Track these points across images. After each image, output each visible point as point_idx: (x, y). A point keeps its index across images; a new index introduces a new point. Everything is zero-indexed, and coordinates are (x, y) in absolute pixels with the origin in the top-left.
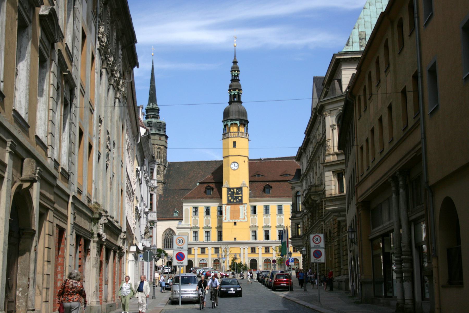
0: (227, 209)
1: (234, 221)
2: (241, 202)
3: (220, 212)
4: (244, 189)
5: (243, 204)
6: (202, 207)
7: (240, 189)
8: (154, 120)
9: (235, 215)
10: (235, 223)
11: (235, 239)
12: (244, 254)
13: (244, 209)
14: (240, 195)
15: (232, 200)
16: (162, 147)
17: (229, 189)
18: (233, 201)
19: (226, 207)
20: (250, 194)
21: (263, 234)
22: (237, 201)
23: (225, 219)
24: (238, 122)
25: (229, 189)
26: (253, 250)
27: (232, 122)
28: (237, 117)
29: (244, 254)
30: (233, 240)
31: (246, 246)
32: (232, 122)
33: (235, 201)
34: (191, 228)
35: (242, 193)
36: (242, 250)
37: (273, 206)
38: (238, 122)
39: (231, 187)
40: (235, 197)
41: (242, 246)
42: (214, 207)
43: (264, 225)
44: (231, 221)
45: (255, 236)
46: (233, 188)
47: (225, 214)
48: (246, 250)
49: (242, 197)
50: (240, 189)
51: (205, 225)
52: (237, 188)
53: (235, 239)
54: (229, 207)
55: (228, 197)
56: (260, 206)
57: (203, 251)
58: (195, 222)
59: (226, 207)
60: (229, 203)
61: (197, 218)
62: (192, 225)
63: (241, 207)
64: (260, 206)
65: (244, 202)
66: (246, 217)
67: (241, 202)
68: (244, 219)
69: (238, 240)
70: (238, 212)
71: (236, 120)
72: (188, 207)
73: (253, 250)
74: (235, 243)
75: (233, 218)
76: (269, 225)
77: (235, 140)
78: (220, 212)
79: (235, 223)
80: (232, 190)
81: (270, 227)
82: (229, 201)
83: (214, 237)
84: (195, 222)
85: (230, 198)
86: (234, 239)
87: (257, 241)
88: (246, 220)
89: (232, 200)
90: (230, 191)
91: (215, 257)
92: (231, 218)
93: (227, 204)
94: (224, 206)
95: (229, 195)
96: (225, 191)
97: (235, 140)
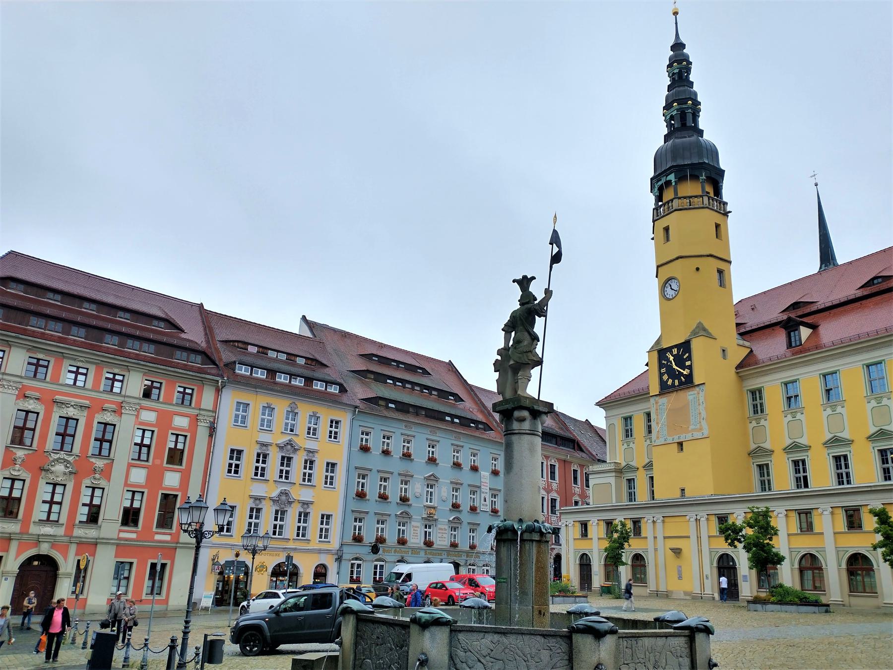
10: (680, 444)
12: (699, 538)
14: (688, 363)
15: (670, 382)
22: (681, 383)
23: (658, 438)
24: (672, 177)
27: (660, 183)
29: (699, 538)
31: (702, 513)
32: (660, 183)
33: (677, 382)
35: (689, 358)
43: (788, 442)
44: (670, 440)
54: (663, 400)
55: (661, 375)
61: (631, 445)
63: (690, 395)
65: (697, 381)
66: (704, 423)
71: (666, 173)
76: (803, 441)
79: (680, 444)
81: (807, 448)
85: (665, 377)
86: (679, 493)
88: (706, 433)
89: (670, 382)
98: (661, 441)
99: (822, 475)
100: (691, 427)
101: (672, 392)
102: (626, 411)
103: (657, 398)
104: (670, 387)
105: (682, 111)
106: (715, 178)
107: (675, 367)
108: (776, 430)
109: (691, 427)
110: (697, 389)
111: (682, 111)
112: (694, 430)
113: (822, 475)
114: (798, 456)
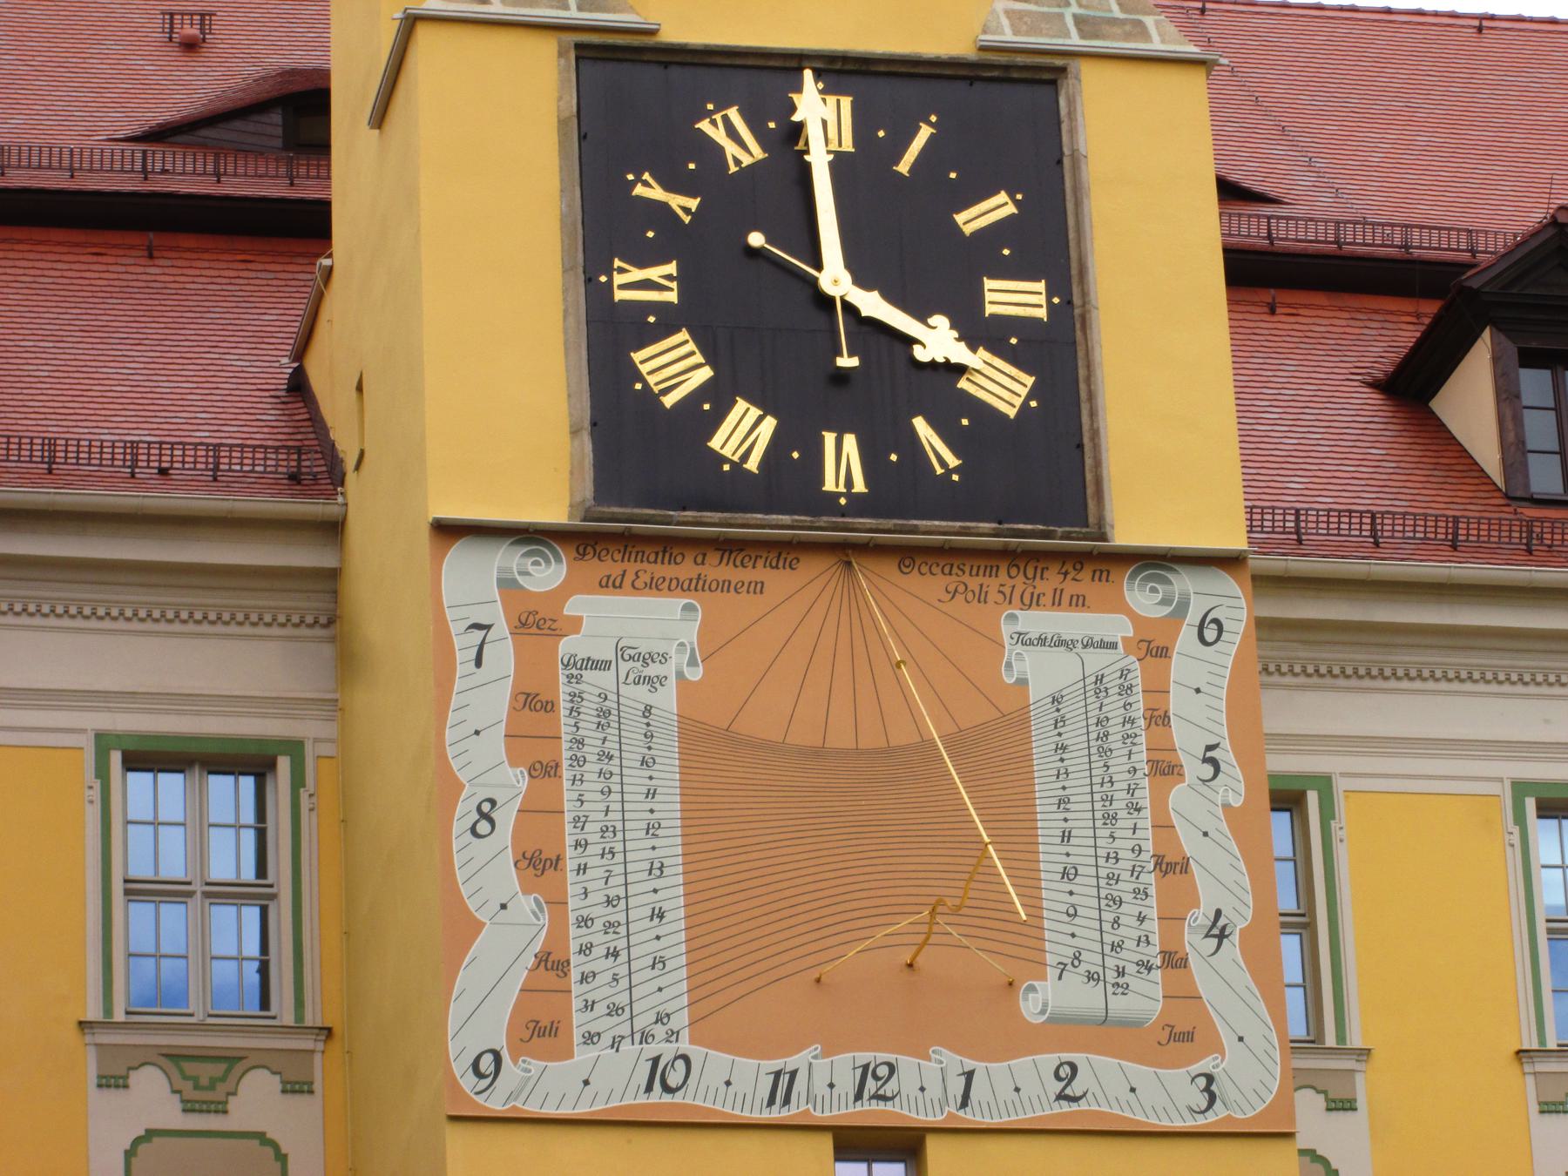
2: (1028, 500)
15: (744, 434)
18: (789, 476)
19: (536, 623)
22: (898, 482)
23: (541, 1030)
33: (843, 462)
47: (538, 864)
55: (611, 334)
59: (536, 623)
60: (648, 494)
67: (1028, 500)
68: (1182, 1034)
80: (735, 140)
85: (674, 368)
90: (691, 162)
92: (726, 989)
95: (646, 282)
98: (605, 1075)
100: (1043, 998)
101: (784, 550)
103: (546, 574)
104: (727, 488)
107: (835, 278)
109: (1043, 998)
110: (1143, 598)
112: (1065, 1029)
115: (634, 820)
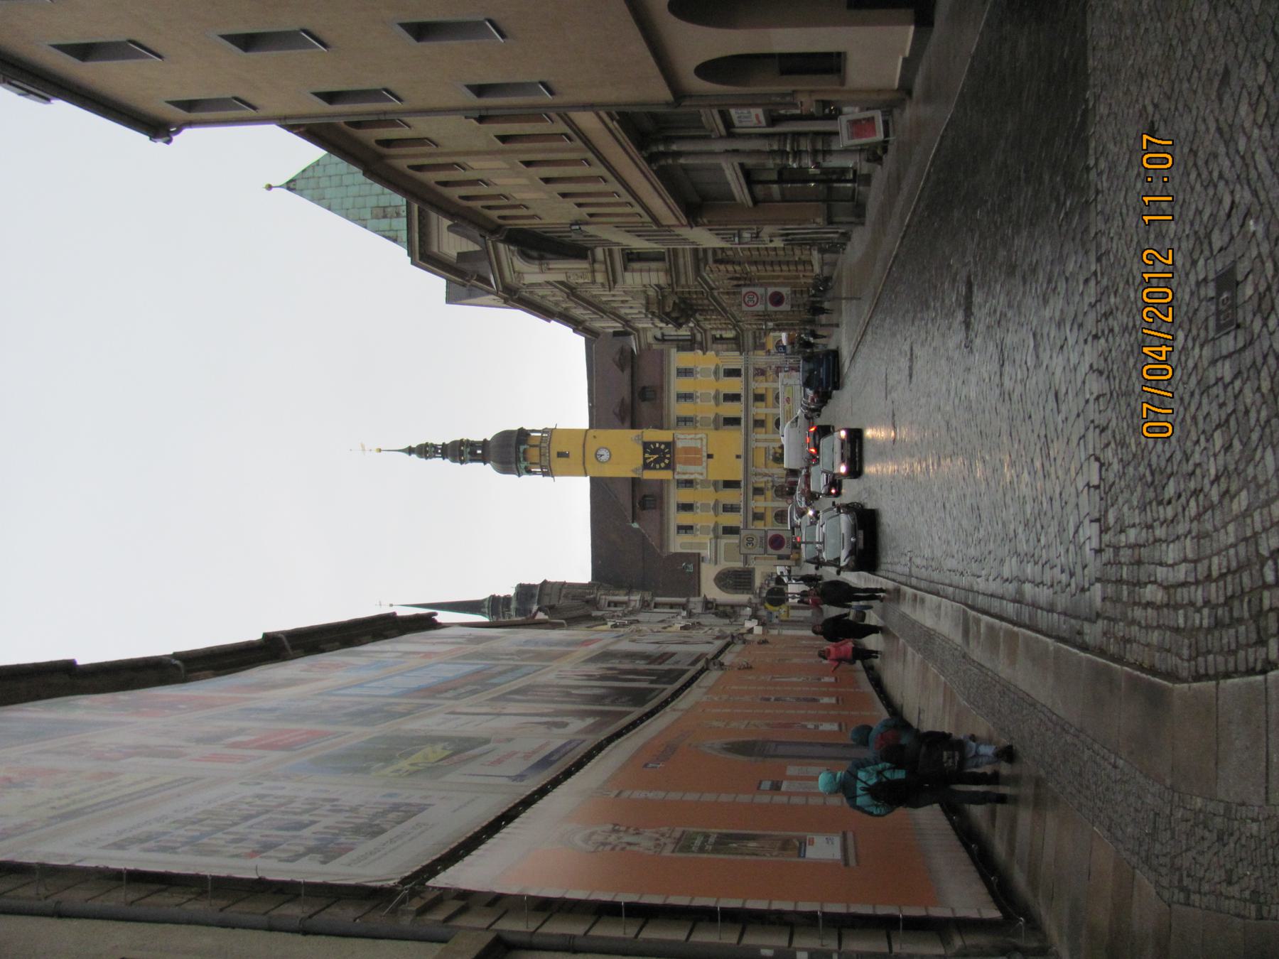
0: (685, 471)
1: (705, 459)
3: (689, 483)
4: (646, 439)
5: (674, 442)
6: (677, 518)
7: (646, 445)
8: (513, 605)
9: (693, 456)
10: (710, 456)
11: (738, 457)
12: (766, 440)
13: (685, 439)
16: (564, 592)
17: (646, 466)
20: (656, 427)
21: (729, 404)
25: (646, 466)
26: (759, 423)
28: (513, 450)
29: (766, 440)
30: (741, 461)
31: (753, 436)
34: (717, 537)
35: (654, 443)
36: (760, 444)
37: (678, 385)
38: (522, 448)
39: (641, 462)
40: (661, 455)
41: (753, 444)
42: (677, 496)
45: (734, 421)
46: (645, 459)
48: (759, 436)
49: (661, 443)
50: (646, 445)
51: (712, 512)
52: (645, 452)
53: (738, 457)
54: (679, 468)
55: (661, 468)
56: (678, 409)
57: (758, 517)
58: (704, 530)
62: (712, 535)
63: (680, 444)
64: (678, 409)
67: (670, 445)
69: (741, 452)
70: (687, 450)
72: (678, 544)
73: (759, 423)
74: (747, 456)
75: (700, 459)
76: (713, 393)
77: (554, 454)
78: (689, 483)
79: (710, 456)
82: (668, 467)
83: (731, 496)
84: (704, 530)
87: (742, 415)
91: (770, 494)
93: (674, 470)
94: (677, 477)
96: (649, 475)
97: (554, 454)
99: (735, 385)
102: (673, 529)
105: (460, 451)
106: (523, 435)
108: (705, 409)
111: (460, 451)
113: (735, 385)
114: (721, 397)
115: (691, 468)
